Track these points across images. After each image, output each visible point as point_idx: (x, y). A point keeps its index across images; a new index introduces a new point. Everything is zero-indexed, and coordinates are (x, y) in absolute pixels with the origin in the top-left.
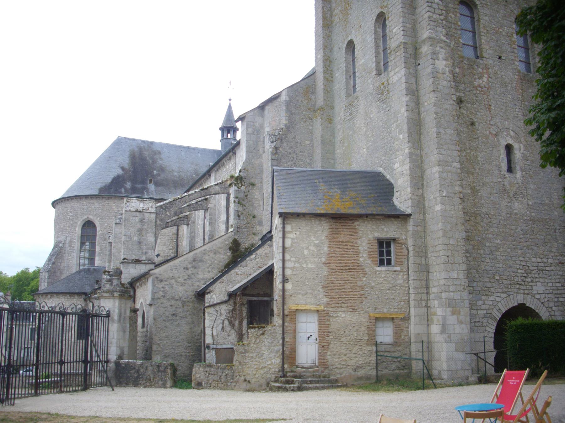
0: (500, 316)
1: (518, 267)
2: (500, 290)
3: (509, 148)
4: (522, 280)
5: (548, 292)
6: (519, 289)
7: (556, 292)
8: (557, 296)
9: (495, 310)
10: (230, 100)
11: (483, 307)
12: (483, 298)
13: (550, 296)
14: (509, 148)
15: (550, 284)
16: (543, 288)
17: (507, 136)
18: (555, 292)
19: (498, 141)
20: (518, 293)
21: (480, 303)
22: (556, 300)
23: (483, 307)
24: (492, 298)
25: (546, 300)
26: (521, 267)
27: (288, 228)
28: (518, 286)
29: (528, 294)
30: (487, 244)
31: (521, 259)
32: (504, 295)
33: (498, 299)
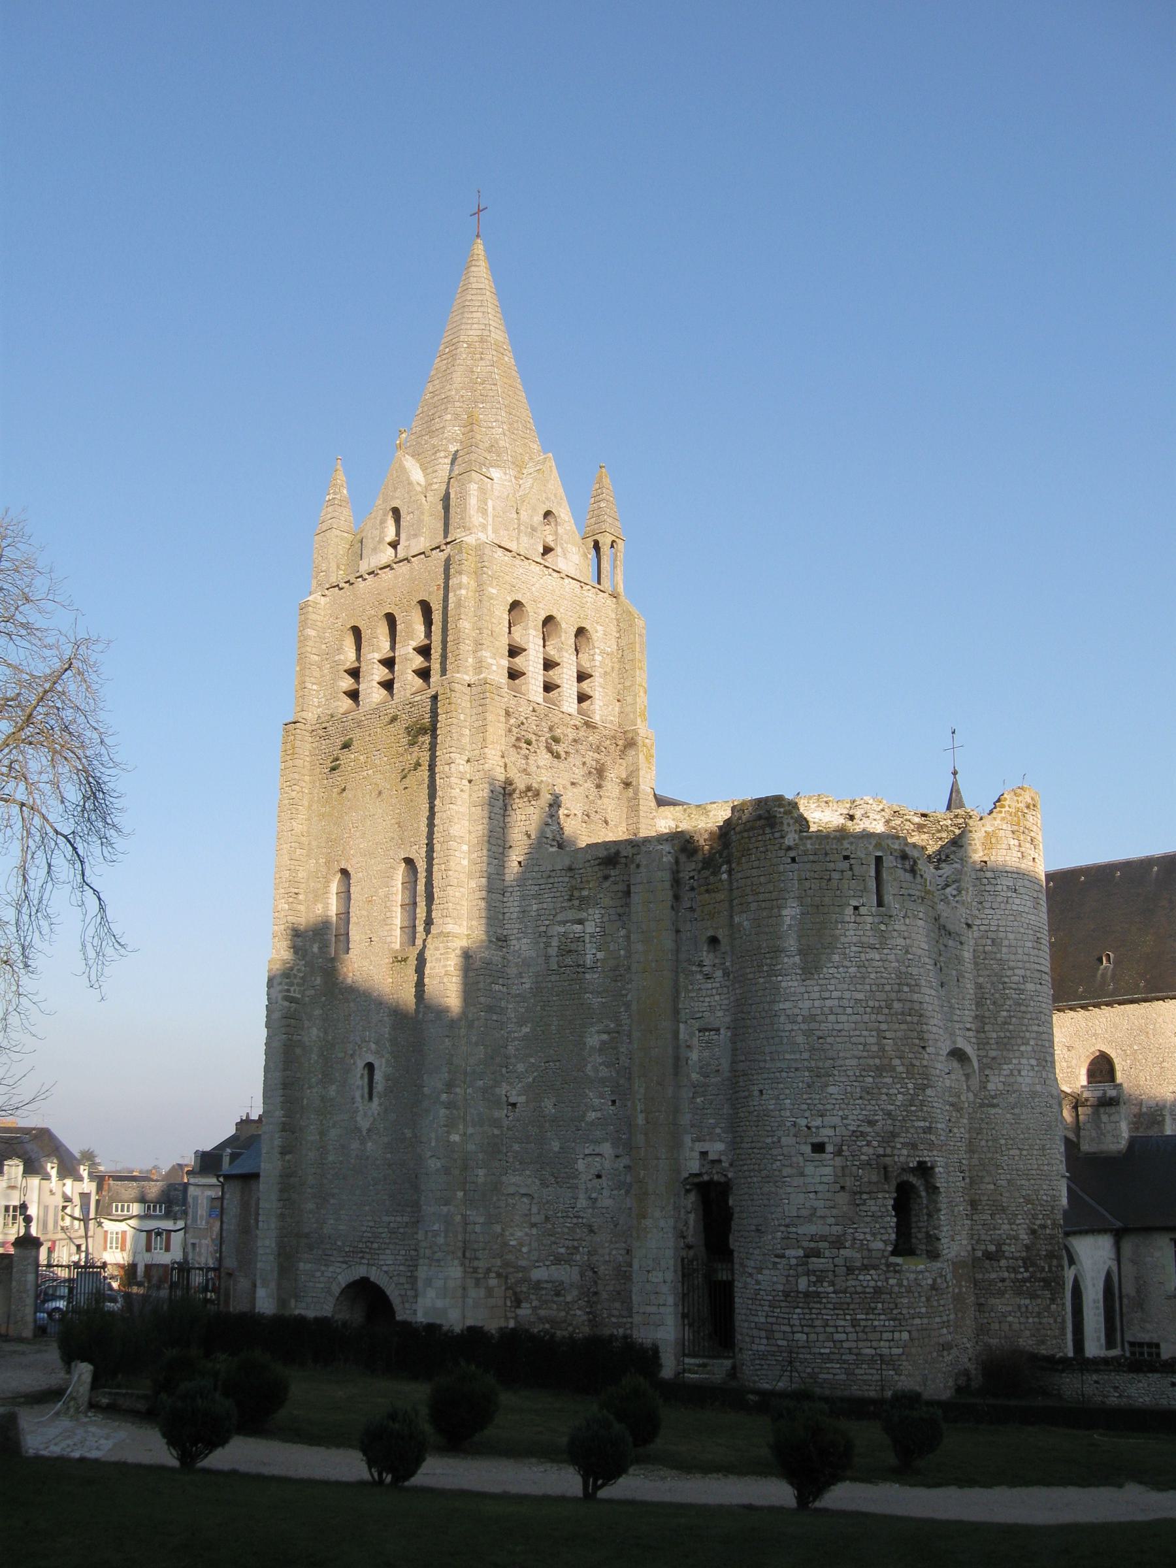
0: (339, 1291)
1: (364, 1229)
2: (341, 1259)
3: (370, 1067)
4: (367, 1247)
5: (398, 1262)
6: (363, 1258)
7: (411, 1263)
8: (411, 1268)
9: (334, 1284)
10: (955, 773)
11: (322, 1279)
12: (323, 1268)
13: (402, 1268)
14: (370, 1067)
15: (403, 1252)
16: (392, 1257)
17: (366, 1052)
18: (407, 1263)
19: (354, 1064)
20: (361, 1263)
21: (318, 1274)
22: (409, 1274)
23: (322, 1279)
24: (331, 1269)
25: (395, 1273)
26: (369, 1229)
27: (226, 1187)
28: (361, 1255)
29: (373, 1265)
30: (332, 1201)
31: (368, 1218)
32: (344, 1266)
33: (338, 1270)
